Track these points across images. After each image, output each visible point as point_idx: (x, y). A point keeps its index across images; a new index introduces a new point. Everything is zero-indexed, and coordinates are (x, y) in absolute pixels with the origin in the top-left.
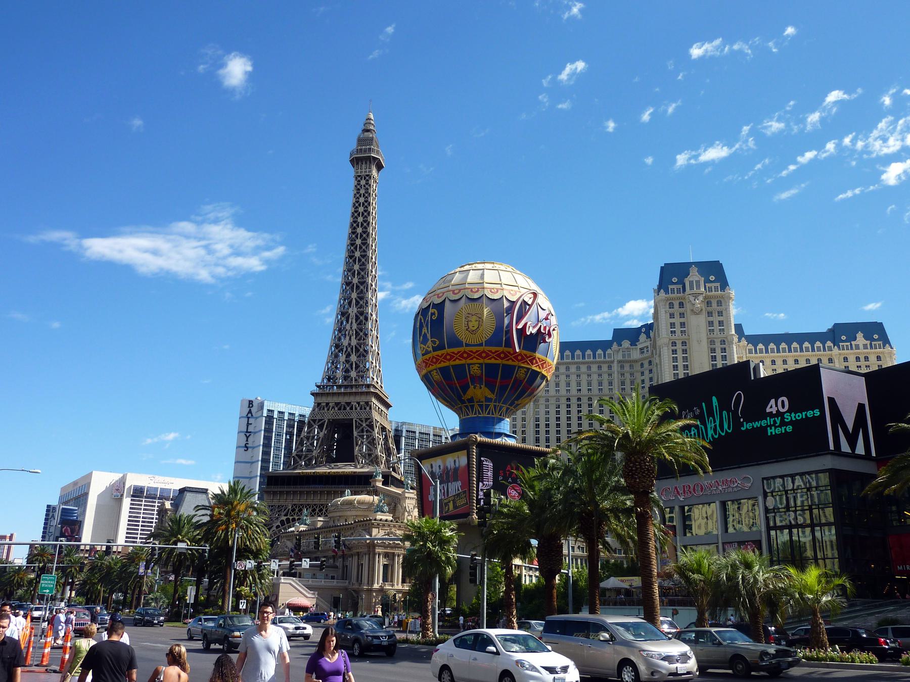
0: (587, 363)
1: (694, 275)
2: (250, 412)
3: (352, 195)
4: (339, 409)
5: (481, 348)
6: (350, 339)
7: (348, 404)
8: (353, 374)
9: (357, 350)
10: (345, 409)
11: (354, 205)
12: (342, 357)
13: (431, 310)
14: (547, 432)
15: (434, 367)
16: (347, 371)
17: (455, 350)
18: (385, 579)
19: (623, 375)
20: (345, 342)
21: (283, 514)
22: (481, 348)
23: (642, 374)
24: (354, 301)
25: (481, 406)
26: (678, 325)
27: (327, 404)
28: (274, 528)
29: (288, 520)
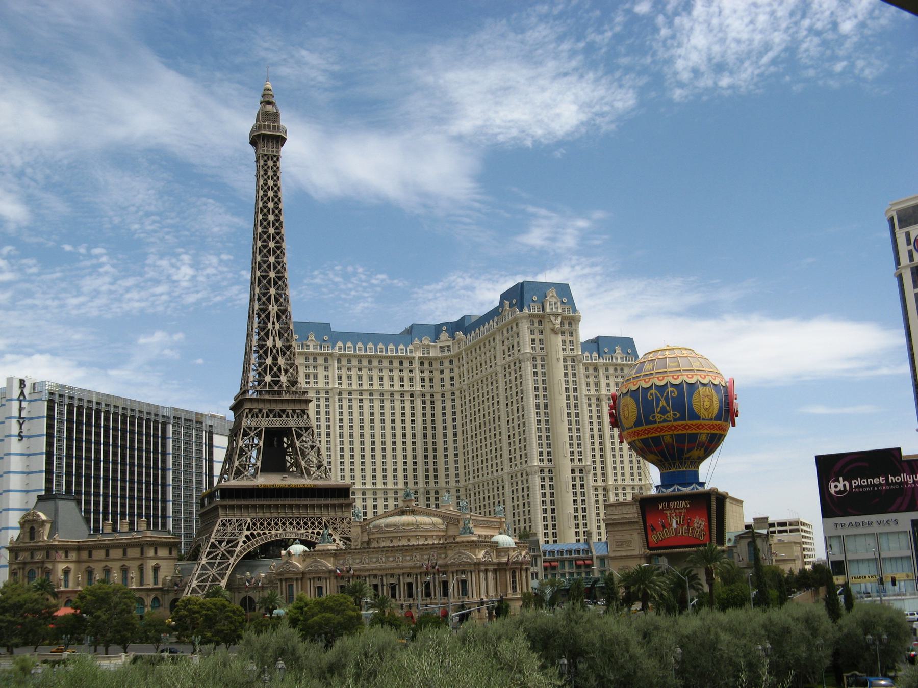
0: (401, 357)
1: (552, 296)
2: (22, 393)
4: (275, 416)
5: (711, 422)
6: (274, 340)
7: (284, 411)
8: (283, 379)
10: (281, 417)
12: (269, 361)
13: (670, 389)
14: (351, 427)
15: (671, 433)
17: (694, 422)
20: (270, 343)
21: (245, 528)
22: (711, 422)
23: (442, 372)
25: (691, 463)
26: (537, 342)
27: (260, 410)
28: (241, 544)
29: (252, 534)
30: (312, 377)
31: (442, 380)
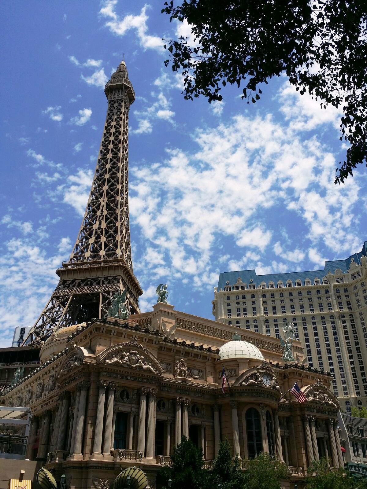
2: (21, 338)
3: (106, 114)
4: (86, 285)
6: (100, 224)
7: (95, 280)
8: (102, 253)
9: (107, 232)
11: (109, 114)
12: (92, 240)
16: (96, 251)
18: (121, 441)
19: (339, 297)
20: (95, 227)
23: (357, 295)
24: (105, 193)
27: (73, 281)
30: (242, 310)
31: (358, 301)
